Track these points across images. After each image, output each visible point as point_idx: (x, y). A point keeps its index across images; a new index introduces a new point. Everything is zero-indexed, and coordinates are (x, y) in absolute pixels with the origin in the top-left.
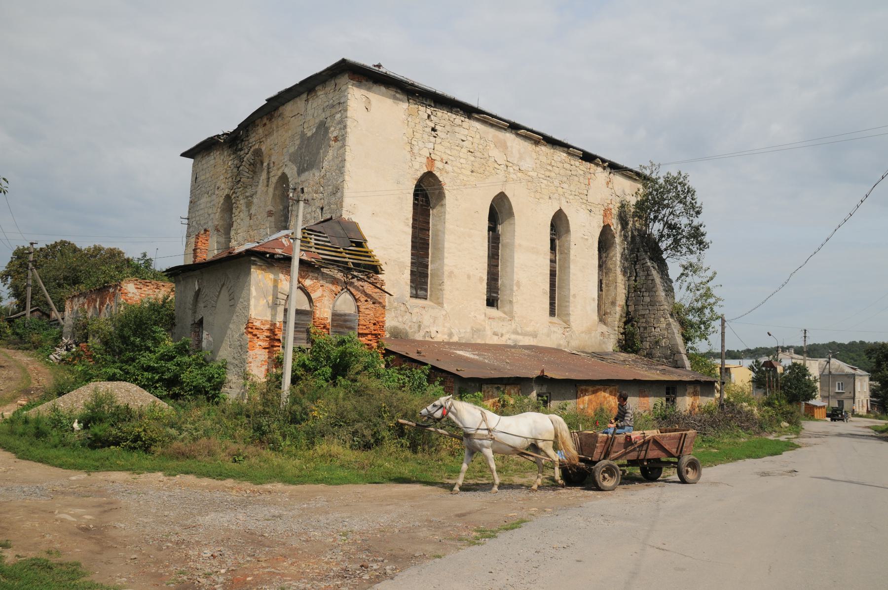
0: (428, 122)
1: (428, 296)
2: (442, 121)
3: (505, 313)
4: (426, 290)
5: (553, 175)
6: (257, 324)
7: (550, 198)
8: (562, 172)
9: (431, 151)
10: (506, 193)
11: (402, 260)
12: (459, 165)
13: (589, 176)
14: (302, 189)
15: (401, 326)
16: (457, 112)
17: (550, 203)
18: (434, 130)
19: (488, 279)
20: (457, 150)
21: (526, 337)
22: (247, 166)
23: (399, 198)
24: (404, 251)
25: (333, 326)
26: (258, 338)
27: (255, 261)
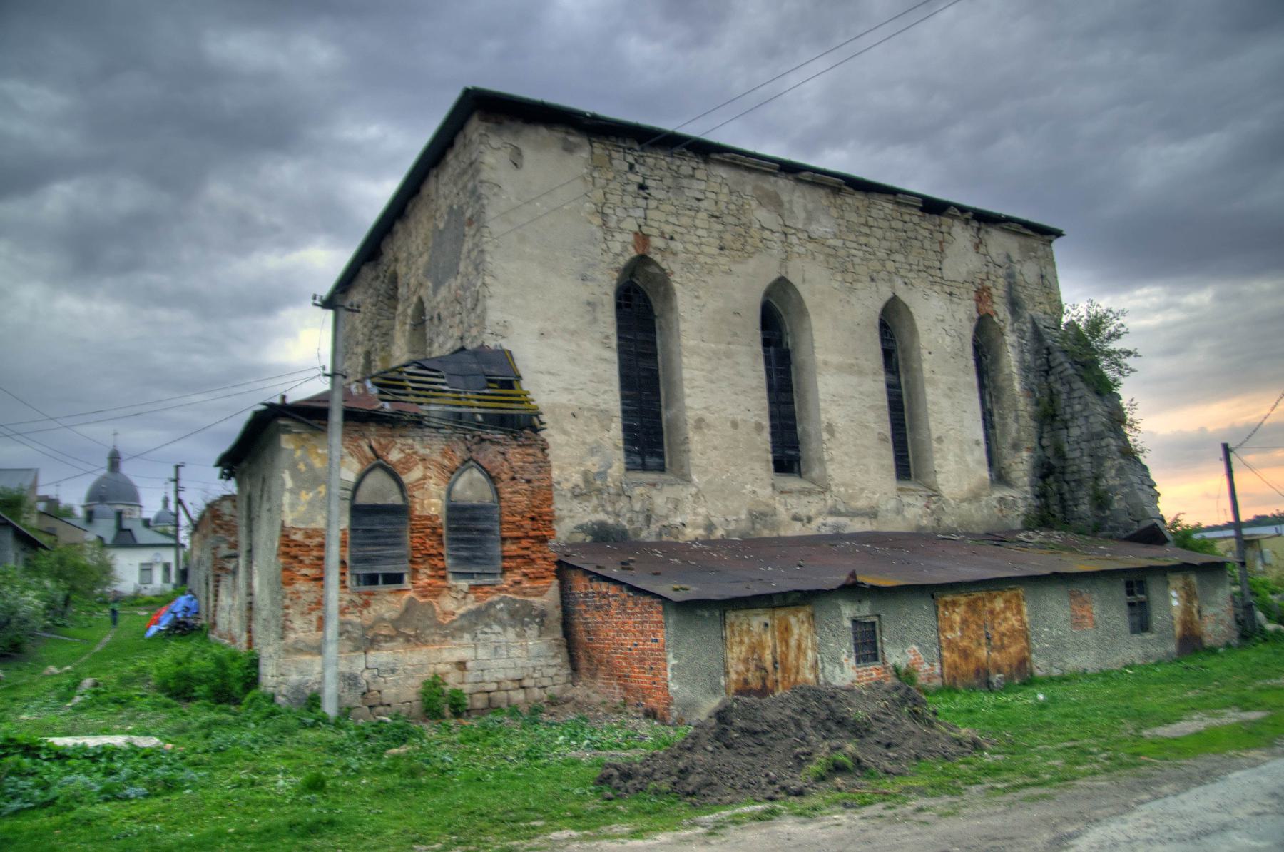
0: (631, 176)
1: (667, 466)
2: (656, 172)
3: (813, 481)
4: (661, 456)
5: (873, 241)
6: (298, 537)
7: (872, 280)
8: (889, 235)
9: (641, 222)
10: (791, 278)
11: (603, 406)
12: (696, 240)
13: (939, 236)
14: (439, 315)
15: (611, 521)
16: (682, 154)
17: (874, 288)
18: (642, 187)
19: (772, 426)
20: (689, 217)
21: (856, 519)
22: (386, 301)
23: (589, 303)
24: (605, 392)
25: (450, 529)
26: (301, 562)
27: (286, 426)
